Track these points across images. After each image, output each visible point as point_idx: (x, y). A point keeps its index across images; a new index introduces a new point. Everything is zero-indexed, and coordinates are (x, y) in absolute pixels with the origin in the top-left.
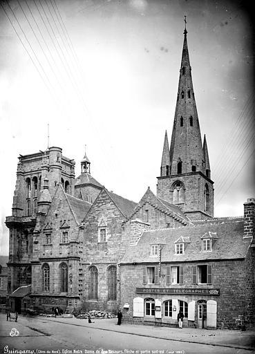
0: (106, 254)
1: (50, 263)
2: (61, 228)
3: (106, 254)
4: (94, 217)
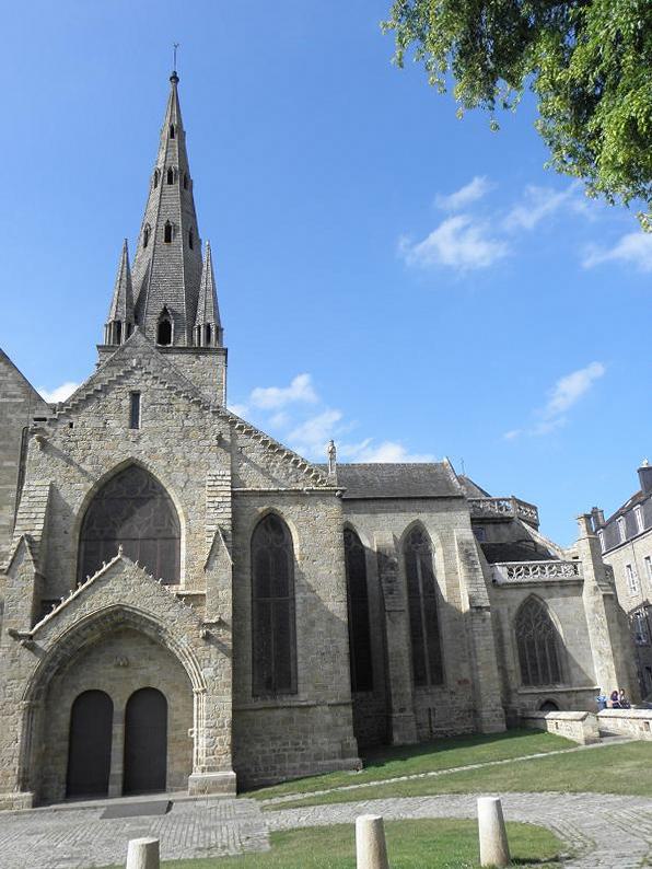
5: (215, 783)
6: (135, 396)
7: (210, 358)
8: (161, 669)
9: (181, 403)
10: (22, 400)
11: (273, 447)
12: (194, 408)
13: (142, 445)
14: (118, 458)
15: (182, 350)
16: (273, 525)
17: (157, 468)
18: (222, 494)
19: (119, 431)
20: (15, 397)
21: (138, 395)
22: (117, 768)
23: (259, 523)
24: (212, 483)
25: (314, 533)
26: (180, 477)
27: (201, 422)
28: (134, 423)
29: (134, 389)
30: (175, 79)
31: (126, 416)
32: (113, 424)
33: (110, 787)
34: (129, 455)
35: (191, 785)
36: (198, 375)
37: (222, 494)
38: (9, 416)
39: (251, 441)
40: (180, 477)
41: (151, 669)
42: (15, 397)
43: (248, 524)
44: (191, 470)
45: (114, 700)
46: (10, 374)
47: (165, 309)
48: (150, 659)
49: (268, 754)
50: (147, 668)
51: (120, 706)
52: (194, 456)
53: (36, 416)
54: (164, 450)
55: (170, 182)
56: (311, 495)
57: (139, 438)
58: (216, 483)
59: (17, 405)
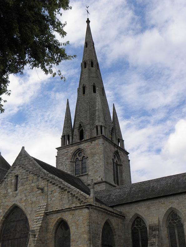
7: (96, 142)
9: (31, 176)
11: (62, 188)
12: (36, 177)
13: (18, 198)
14: (10, 204)
16: (63, 225)
17: (22, 205)
19: (11, 193)
21: (18, 176)
23: (59, 225)
24: (38, 210)
25: (77, 228)
26: (29, 209)
28: (16, 190)
29: (16, 174)
30: (88, 22)
31: (13, 186)
32: (9, 190)
34: (13, 203)
36: (92, 151)
39: (56, 187)
40: (29, 209)
43: (52, 226)
44: (33, 205)
47: (80, 125)
52: (34, 199)
54: (25, 198)
55: (85, 67)
56: (77, 209)
57: (17, 194)
58: (41, 210)
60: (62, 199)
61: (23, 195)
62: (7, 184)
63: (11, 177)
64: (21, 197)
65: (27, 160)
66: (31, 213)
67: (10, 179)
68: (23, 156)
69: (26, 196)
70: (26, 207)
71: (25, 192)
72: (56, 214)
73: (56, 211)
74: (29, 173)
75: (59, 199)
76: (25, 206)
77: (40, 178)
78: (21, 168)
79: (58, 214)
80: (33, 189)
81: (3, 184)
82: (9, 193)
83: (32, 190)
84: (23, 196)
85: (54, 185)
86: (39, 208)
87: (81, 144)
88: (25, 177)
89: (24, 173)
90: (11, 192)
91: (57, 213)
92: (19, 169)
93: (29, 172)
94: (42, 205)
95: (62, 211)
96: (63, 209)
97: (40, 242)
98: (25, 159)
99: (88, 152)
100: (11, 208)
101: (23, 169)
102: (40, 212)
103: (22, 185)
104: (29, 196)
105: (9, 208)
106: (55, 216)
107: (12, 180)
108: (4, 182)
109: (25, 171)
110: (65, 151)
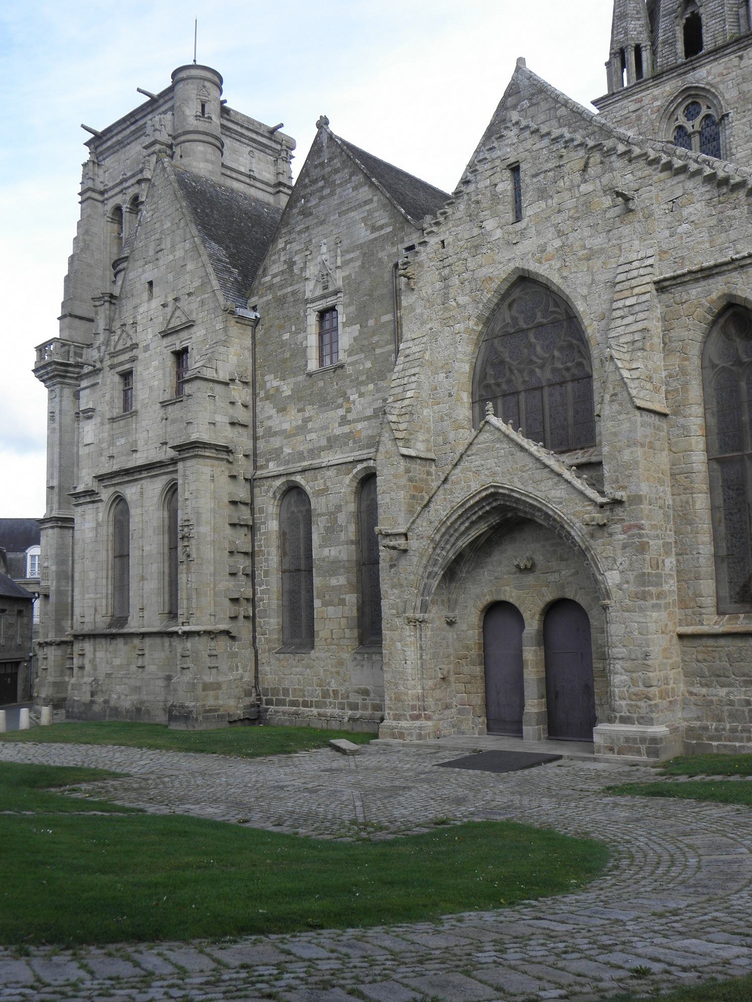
0: (344, 421)
1: (130, 492)
2: (165, 334)
3: (344, 421)
4: (291, 264)
5: (627, 740)
6: (515, 169)
8: (577, 573)
10: (390, 229)
13: (528, 245)
15: (719, 51)
18: (636, 291)
20: (381, 227)
22: (533, 705)
24: (621, 277)
26: (582, 277)
27: (605, 180)
29: (512, 160)
32: (489, 224)
33: (524, 727)
34: (512, 266)
35: (597, 738)
37: (636, 291)
38: (380, 255)
39: (690, 184)
41: (563, 572)
42: (381, 227)
44: (597, 263)
45: (524, 616)
46: (375, 199)
48: (562, 559)
49: (737, 707)
50: (559, 571)
51: (532, 625)
52: (598, 241)
53: (407, 245)
54: (557, 243)
57: (522, 233)
59: (385, 238)
60: (725, 223)
61: (550, 233)
62: (478, 202)
63: (490, 173)
64: (542, 242)
65: (544, 105)
66: (589, 293)
67: (488, 182)
68: (525, 93)
69: (560, 234)
70: (565, 274)
71: (559, 219)
72: (703, 283)
73: (702, 270)
74: (565, 148)
75: (707, 224)
76: (559, 269)
77: (614, 158)
78: (527, 134)
79: (711, 281)
80: (587, 205)
81: (462, 207)
82: (489, 234)
83: (586, 207)
84: (550, 236)
85: (682, 177)
86: (627, 268)
87: (694, 69)
88: (551, 165)
89: (545, 151)
90: (499, 230)
91: (705, 278)
92: (522, 137)
93: (566, 142)
94: (634, 256)
95: (731, 267)
96: (737, 260)
97: (649, 386)
98: (534, 101)
99: (728, 94)
100: (506, 286)
101: (536, 137)
102: (634, 283)
103: (543, 194)
104: (575, 234)
105: (494, 286)
106: (699, 289)
107: (496, 185)
108: (466, 197)
109: (546, 142)
110: (629, 105)
